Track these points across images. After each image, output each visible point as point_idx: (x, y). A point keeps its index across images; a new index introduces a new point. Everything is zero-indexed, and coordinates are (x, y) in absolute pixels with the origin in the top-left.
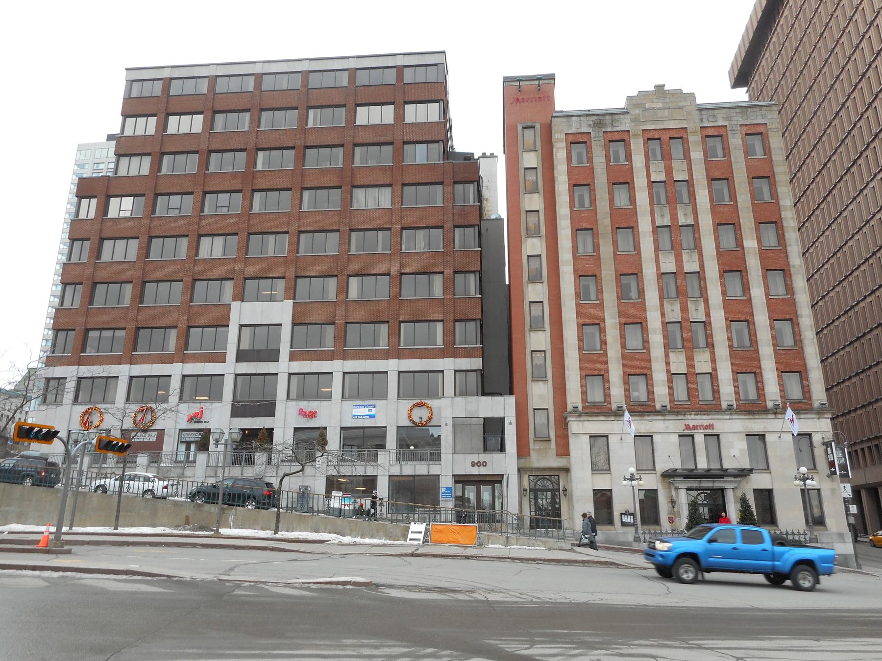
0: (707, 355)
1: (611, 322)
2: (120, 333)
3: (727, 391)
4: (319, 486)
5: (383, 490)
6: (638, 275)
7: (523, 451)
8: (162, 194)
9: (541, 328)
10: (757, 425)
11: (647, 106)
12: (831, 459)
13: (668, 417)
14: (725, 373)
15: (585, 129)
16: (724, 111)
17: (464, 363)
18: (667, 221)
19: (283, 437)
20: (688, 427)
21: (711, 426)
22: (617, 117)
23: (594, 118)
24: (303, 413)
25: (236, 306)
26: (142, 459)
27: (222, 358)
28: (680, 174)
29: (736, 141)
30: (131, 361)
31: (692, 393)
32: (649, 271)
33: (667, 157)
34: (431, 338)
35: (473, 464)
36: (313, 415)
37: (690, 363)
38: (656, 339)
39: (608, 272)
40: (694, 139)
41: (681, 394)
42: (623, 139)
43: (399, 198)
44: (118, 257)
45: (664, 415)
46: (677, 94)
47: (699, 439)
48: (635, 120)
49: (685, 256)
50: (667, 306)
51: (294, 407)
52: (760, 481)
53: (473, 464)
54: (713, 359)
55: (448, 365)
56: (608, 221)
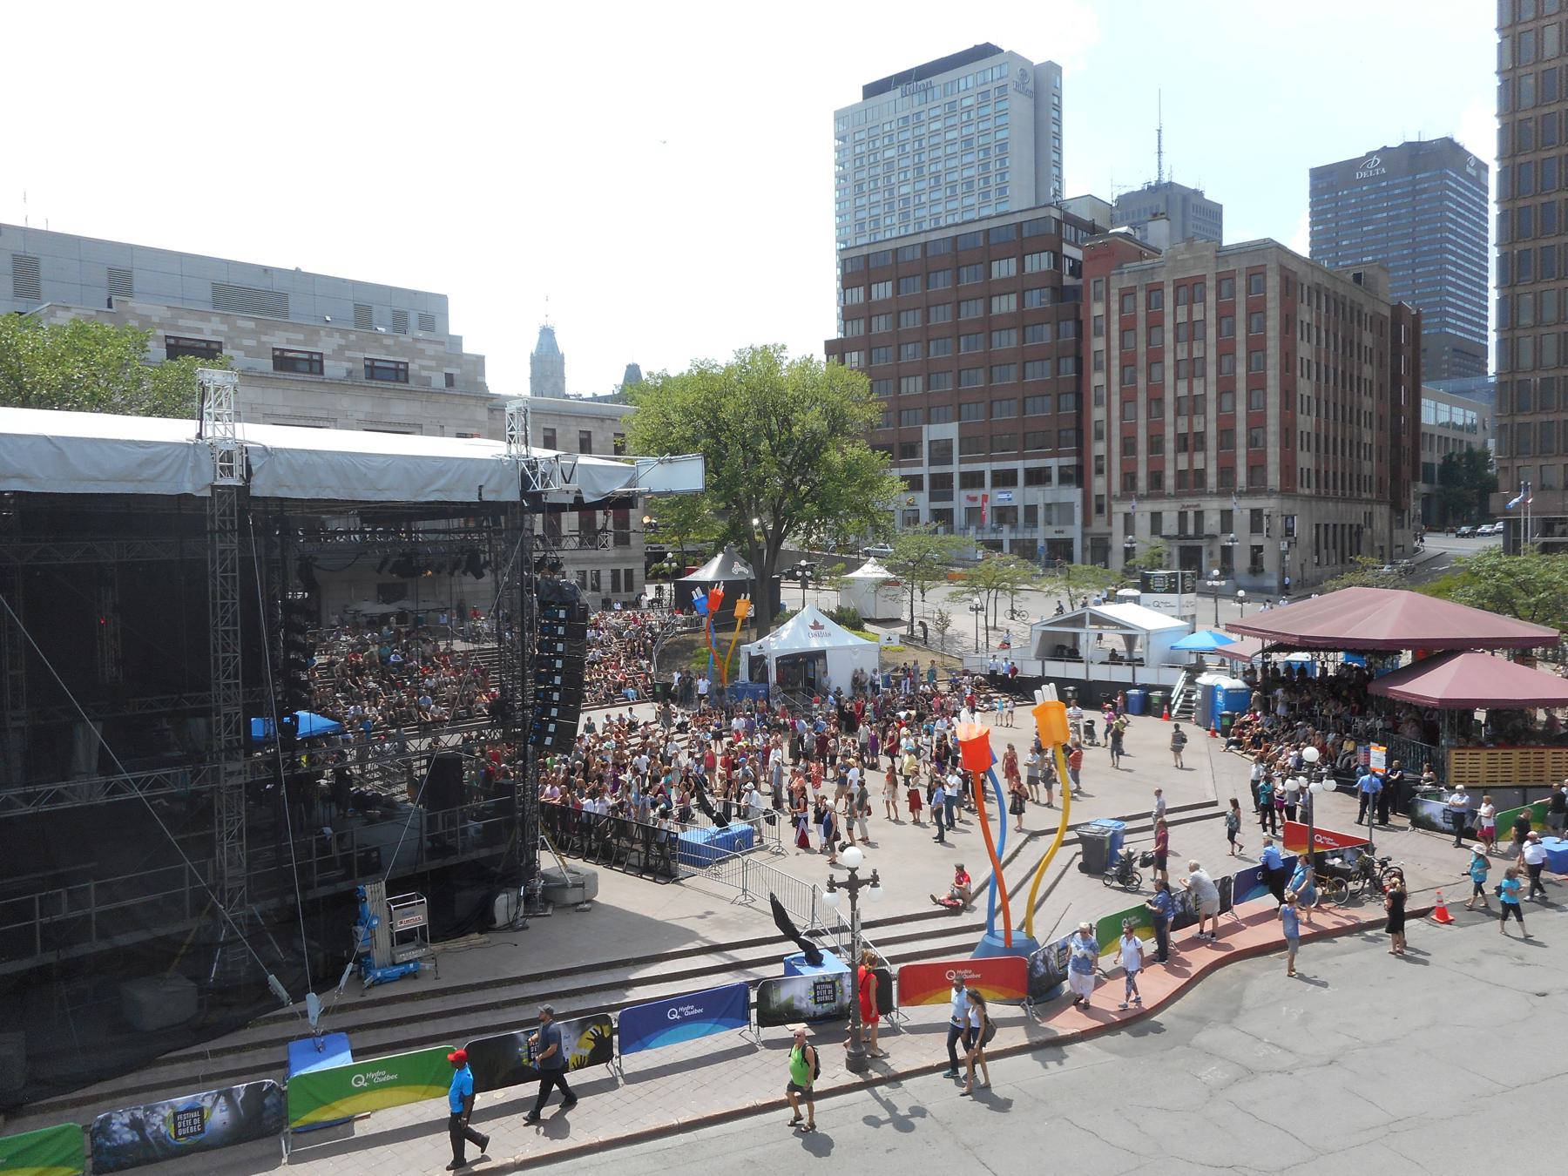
7: (1086, 522)
10: (1228, 504)
11: (1179, 258)
12: (1290, 526)
17: (1065, 461)
18: (1185, 356)
19: (959, 517)
20: (1183, 506)
21: (1198, 506)
25: (925, 427)
27: (920, 464)
28: (1197, 316)
35: (1056, 532)
52: (1225, 541)
53: (1056, 532)
54: (1206, 459)
55: (1053, 463)
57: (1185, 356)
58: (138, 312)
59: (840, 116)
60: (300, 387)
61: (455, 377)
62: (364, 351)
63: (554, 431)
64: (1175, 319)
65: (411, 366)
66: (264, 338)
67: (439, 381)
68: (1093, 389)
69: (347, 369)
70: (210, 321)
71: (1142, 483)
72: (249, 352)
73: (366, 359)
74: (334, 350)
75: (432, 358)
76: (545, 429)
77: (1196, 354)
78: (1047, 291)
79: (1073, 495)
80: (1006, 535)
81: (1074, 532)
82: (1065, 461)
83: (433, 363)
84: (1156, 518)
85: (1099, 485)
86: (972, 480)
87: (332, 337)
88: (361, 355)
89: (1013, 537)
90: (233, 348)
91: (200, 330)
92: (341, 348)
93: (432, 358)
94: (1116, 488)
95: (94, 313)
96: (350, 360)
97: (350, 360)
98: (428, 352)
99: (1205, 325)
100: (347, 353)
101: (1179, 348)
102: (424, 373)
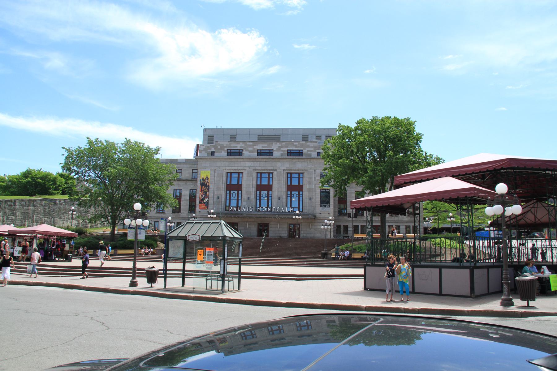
58: (220, 144)
60: (265, 160)
62: (287, 148)
65: (304, 151)
66: (255, 147)
69: (281, 154)
70: (239, 144)
72: (251, 152)
73: (288, 150)
74: (277, 148)
75: (312, 147)
83: (313, 149)
88: (286, 149)
90: (245, 151)
91: (237, 147)
92: (280, 147)
93: (312, 147)
95: (209, 146)
96: (282, 151)
97: (282, 151)
98: (310, 146)
100: (282, 149)
102: (309, 153)
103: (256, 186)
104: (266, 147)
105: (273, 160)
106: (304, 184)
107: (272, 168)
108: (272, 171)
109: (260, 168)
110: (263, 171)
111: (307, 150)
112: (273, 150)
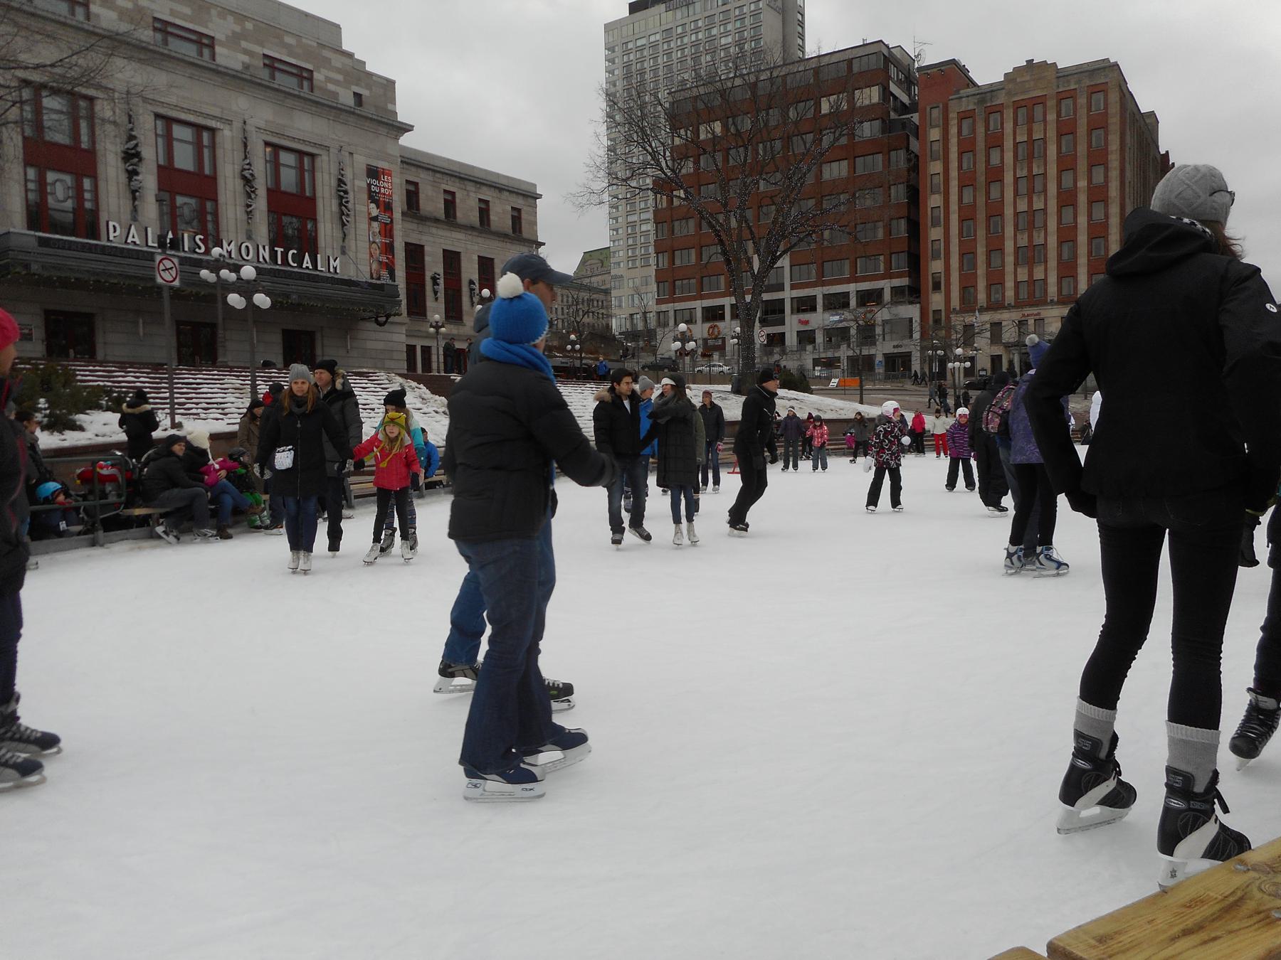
0: (1042, 268)
1: (981, 250)
2: (693, 281)
3: (1052, 290)
4: (809, 363)
5: (844, 364)
6: (1001, 215)
8: (702, 185)
9: (939, 258)
11: (1018, 80)
13: (1012, 310)
14: (1052, 279)
15: (971, 107)
16: (1076, 76)
17: (897, 282)
18: (1025, 173)
19: (791, 340)
20: (1024, 315)
21: (1039, 314)
22: (994, 93)
23: (978, 96)
24: (801, 322)
26: (716, 356)
29: (1082, 101)
30: (702, 298)
31: (1032, 294)
32: (1009, 212)
33: (1031, 120)
34: (876, 268)
35: (894, 347)
36: (807, 322)
37: (1031, 274)
38: (1010, 259)
39: (981, 215)
40: (1051, 103)
41: (1024, 294)
42: (999, 109)
43: (853, 168)
44: (685, 233)
45: (1009, 309)
46: (1044, 64)
47: (1031, 322)
48: (1009, 93)
49: (1035, 199)
50: (1019, 236)
51: (796, 317)
53: (894, 347)
54: (1046, 270)
55: (886, 285)
56: (983, 179)
57: (1025, 173)
59: (609, 28)
61: (363, 97)
62: (262, 45)
63: (453, 194)
64: (1015, 139)
65: (316, 75)
67: (347, 99)
68: (929, 210)
71: (982, 297)
73: (265, 56)
74: (227, 37)
75: (338, 71)
76: (445, 191)
77: (1035, 171)
78: (877, 123)
79: (911, 311)
80: (844, 353)
81: (913, 346)
82: (897, 282)
84: (996, 327)
85: (937, 301)
86: (806, 305)
87: (225, 19)
88: (259, 50)
89: (850, 353)
93: (338, 71)
94: (955, 302)
96: (246, 52)
97: (246, 52)
98: (334, 63)
99: (1045, 143)
100: (244, 44)
101: (1018, 165)
102: (331, 87)
103: (155, 171)
104: (184, 17)
105: (220, 80)
106: (319, 194)
107: (217, 112)
108: (213, 124)
109: (173, 100)
110: (183, 116)
111: (326, 77)
112: (213, 38)
